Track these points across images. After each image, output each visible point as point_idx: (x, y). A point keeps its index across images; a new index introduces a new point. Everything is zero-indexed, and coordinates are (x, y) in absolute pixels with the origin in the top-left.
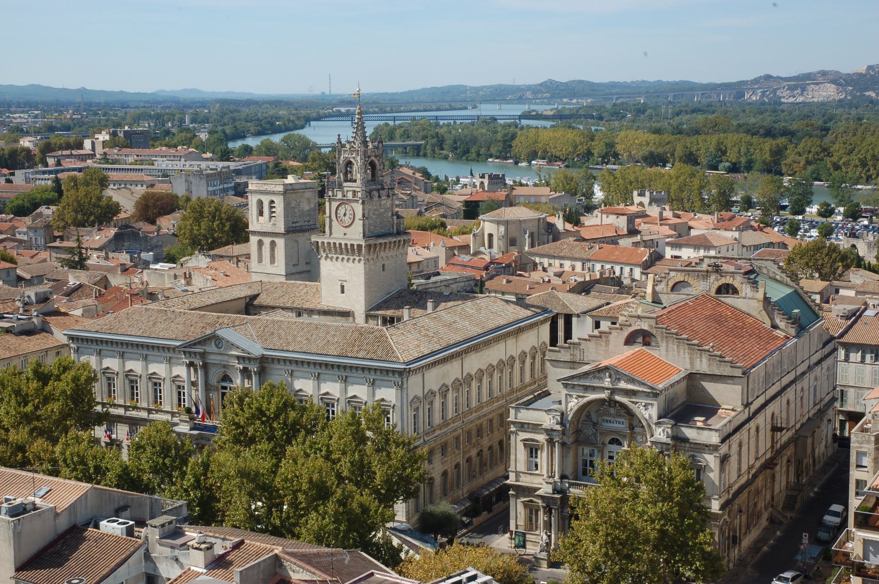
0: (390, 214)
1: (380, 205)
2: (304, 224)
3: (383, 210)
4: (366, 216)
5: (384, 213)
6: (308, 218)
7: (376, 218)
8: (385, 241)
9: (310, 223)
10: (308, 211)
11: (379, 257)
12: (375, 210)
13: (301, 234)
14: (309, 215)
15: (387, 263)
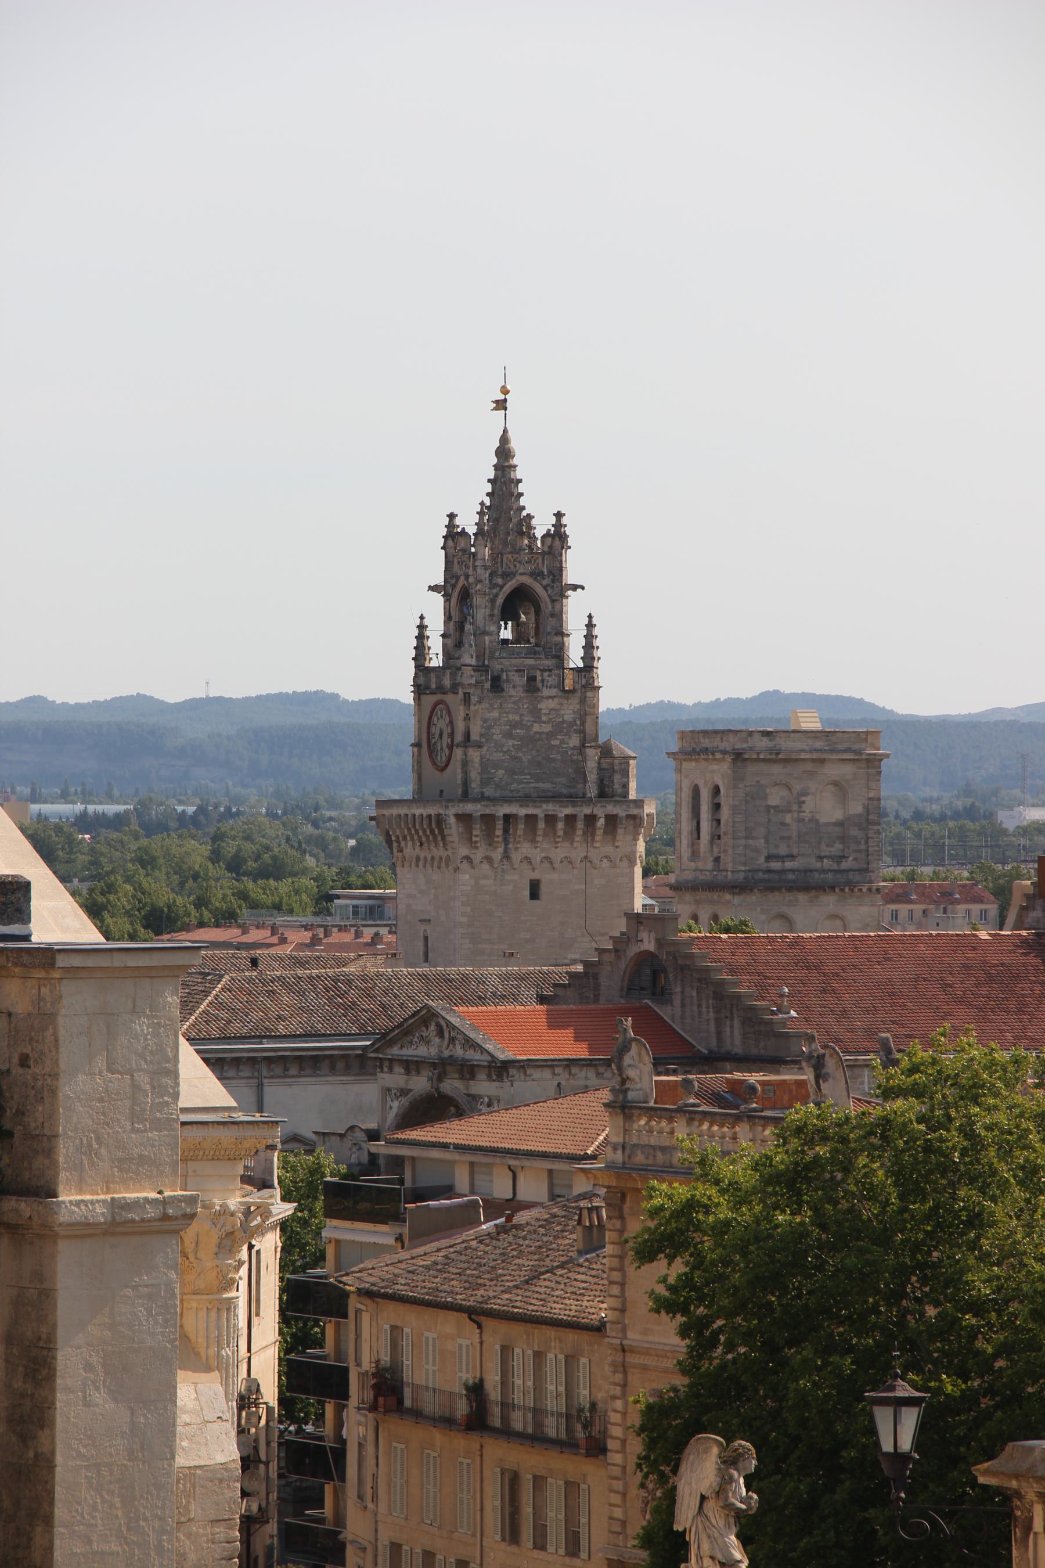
0: (575, 741)
1: (536, 713)
2: (819, 865)
3: (547, 728)
4: (474, 737)
5: (551, 735)
6: (837, 848)
7: (518, 748)
8: (531, 811)
9: (844, 865)
10: (841, 824)
11: (516, 857)
12: (514, 725)
13: (802, 897)
14: (842, 839)
15: (547, 878)
